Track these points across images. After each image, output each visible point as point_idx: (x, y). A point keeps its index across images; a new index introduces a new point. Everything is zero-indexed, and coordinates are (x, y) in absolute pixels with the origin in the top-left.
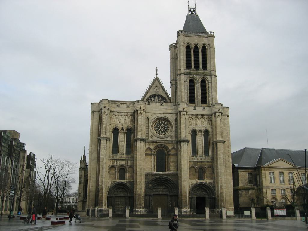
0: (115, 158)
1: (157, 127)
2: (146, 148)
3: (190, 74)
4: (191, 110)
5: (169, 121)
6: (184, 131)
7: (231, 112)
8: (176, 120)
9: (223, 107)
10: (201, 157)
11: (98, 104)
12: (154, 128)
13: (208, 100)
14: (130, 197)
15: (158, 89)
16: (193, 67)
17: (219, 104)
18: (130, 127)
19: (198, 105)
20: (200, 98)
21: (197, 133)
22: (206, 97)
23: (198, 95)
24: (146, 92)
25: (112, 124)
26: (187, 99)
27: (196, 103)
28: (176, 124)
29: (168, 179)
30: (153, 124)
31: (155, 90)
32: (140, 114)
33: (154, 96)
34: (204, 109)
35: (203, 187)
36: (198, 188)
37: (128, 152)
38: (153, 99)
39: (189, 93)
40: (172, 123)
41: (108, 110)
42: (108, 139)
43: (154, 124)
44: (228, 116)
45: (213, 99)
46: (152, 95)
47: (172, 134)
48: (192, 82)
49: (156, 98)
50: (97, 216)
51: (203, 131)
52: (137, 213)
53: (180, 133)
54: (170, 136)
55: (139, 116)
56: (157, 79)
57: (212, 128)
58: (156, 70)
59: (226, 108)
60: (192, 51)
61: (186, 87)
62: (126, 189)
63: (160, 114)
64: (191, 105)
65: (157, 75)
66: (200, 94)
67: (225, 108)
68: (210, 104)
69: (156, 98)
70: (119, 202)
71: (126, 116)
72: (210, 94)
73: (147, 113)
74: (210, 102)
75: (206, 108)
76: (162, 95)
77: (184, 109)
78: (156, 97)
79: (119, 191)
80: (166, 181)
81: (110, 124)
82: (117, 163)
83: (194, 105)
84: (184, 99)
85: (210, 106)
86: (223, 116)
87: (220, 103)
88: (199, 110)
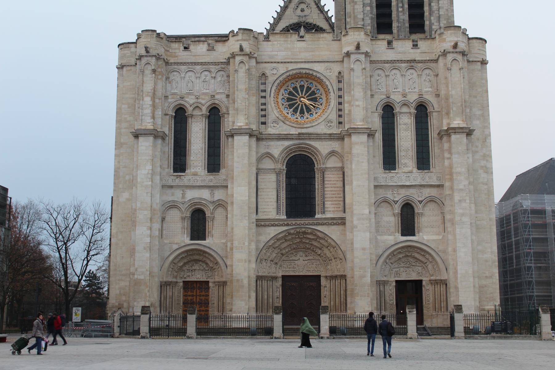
0: (177, 182)
1: (289, 100)
2: (259, 155)
4: (380, 48)
5: (320, 81)
6: (358, 106)
7: (491, 53)
8: (340, 78)
9: (469, 39)
10: (409, 174)
11: (133, 45)
12: (280, 100)
13: (427, 23)
14: (219, 282)
15: (306, 9)
17: (457, 29)
18: (217, 102)
19: (401, 37)
20: (406, 17)
21: (397, 110)
22: (422, 15)
23: (400, 9)
24: (275, 17)
25: (170, 97)
26: (369, 21)
27: (395, 30)
28: (340, 89)
29: (319, 234)
30: (279, 90)
31: (298, 12)
32: (242, 65)
33: (295, 28)
34: (415, 46)
35: (417, 256)
36: (401, 256)
39: (374, 5)
40: (330, 87)
41: (158, 57)
42: (156, 135)
43: (282, 91)
44: (484, 63)
45: (441, 19)
46: (291, 25)
47: (330, 115)
50: (120, 335)
51: (414, 105)
52: (235, 325)
53: (350, 111)
54: (321, 122)
55: (239, 70)
57: (438, 96)
59: (478, 41)
62: (208, 262)
63: (295, 64)
64: (381, 36)
66: (406, 6)
67: (474, 41)
68: (433, 32)
70: (193, 296)
71: (206, 73)
72: (432, 4)
73: (262, 62)
74: (434, 27)
75: (420, 43)
76: (318, 24)
77: (358, 47)
78: (302, 29)
79: (193, 268)
80: (316, 240)
81: (166, 97)
82: (183, 197)
83: (388, 37)
84: (362, 23)
85: (433, 36)
86: (468, 61)
87: (460, 27)
88: (403, 48)
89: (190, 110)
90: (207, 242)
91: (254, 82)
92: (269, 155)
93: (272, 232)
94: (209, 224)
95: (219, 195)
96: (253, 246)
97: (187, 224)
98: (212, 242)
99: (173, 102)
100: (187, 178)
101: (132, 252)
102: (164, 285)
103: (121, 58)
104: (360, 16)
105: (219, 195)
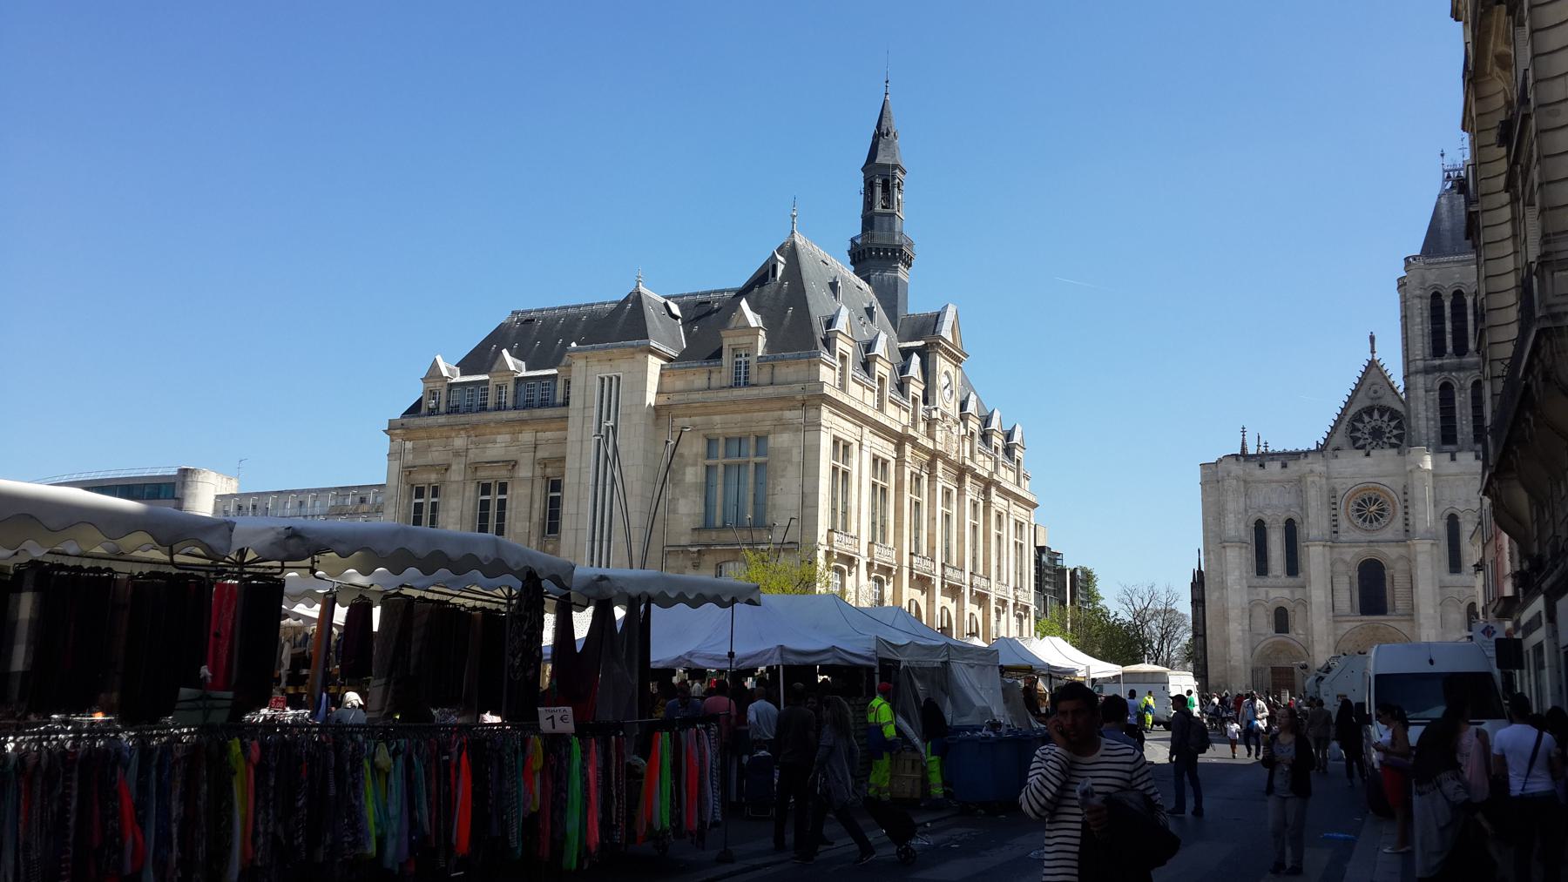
3: (1441, 368)
16: (1450, 349)
20: (1471, 429)
26: (1432, 435)
33: (1369, 411)
37: (1293, 567)
38: (1366, 419)
48: (1446, 391)
49: (1376, 415)
56: (1372, 364)
58: (1372, 339)
60: (1447, 304)
61: (1430, 403)
65: (1373, 352)
69: (1376, 415)
83: (1452, 447)
89: (1268, 521)
90: (1292, 634)
91: (1325, 499)
92: (1344, 561)
93: (1347, 626)
94: (1291, 620)
95: (1298, 594)
96: (1331, 640)
97: (1272, 618)
98: (1297, 633)
99: (1254, 517)
100: (1269, 580)
101: (1226, 643)
102: (1254, 671)
103: (1203, 476)
104: (1424, 431)
105: (1298, 594)
